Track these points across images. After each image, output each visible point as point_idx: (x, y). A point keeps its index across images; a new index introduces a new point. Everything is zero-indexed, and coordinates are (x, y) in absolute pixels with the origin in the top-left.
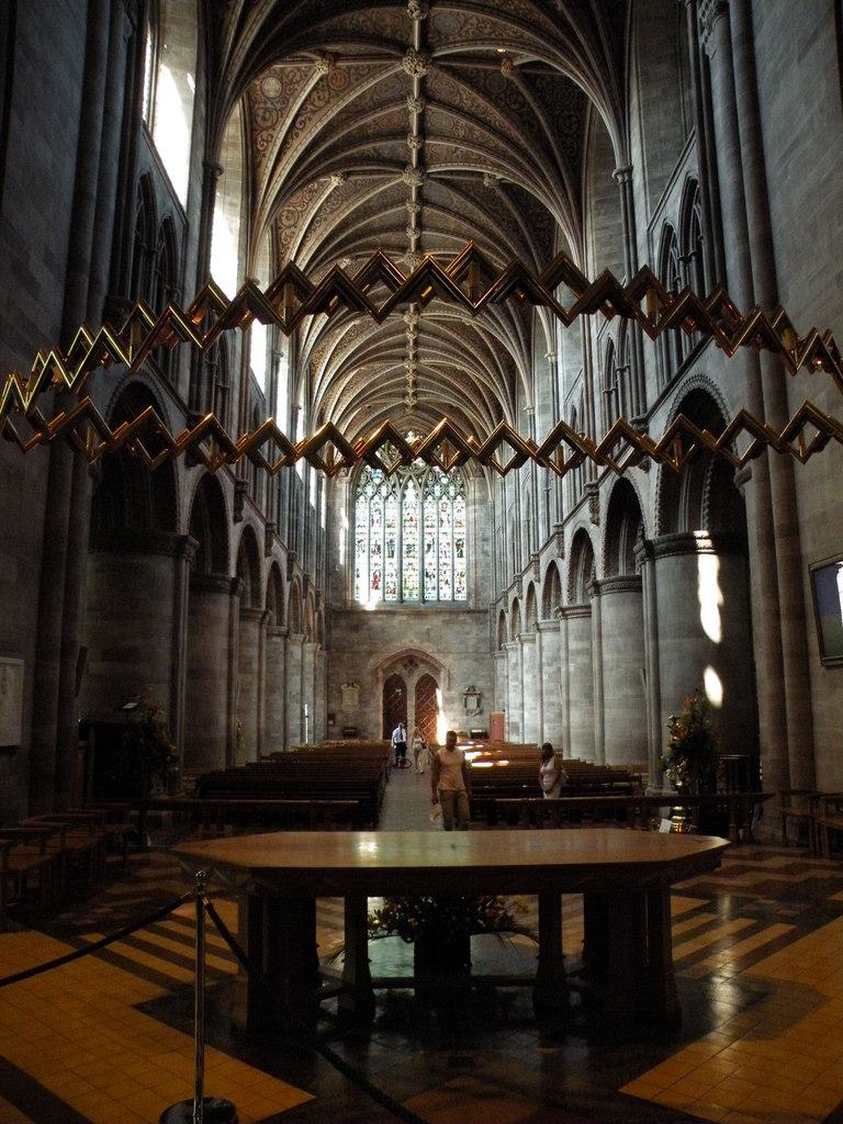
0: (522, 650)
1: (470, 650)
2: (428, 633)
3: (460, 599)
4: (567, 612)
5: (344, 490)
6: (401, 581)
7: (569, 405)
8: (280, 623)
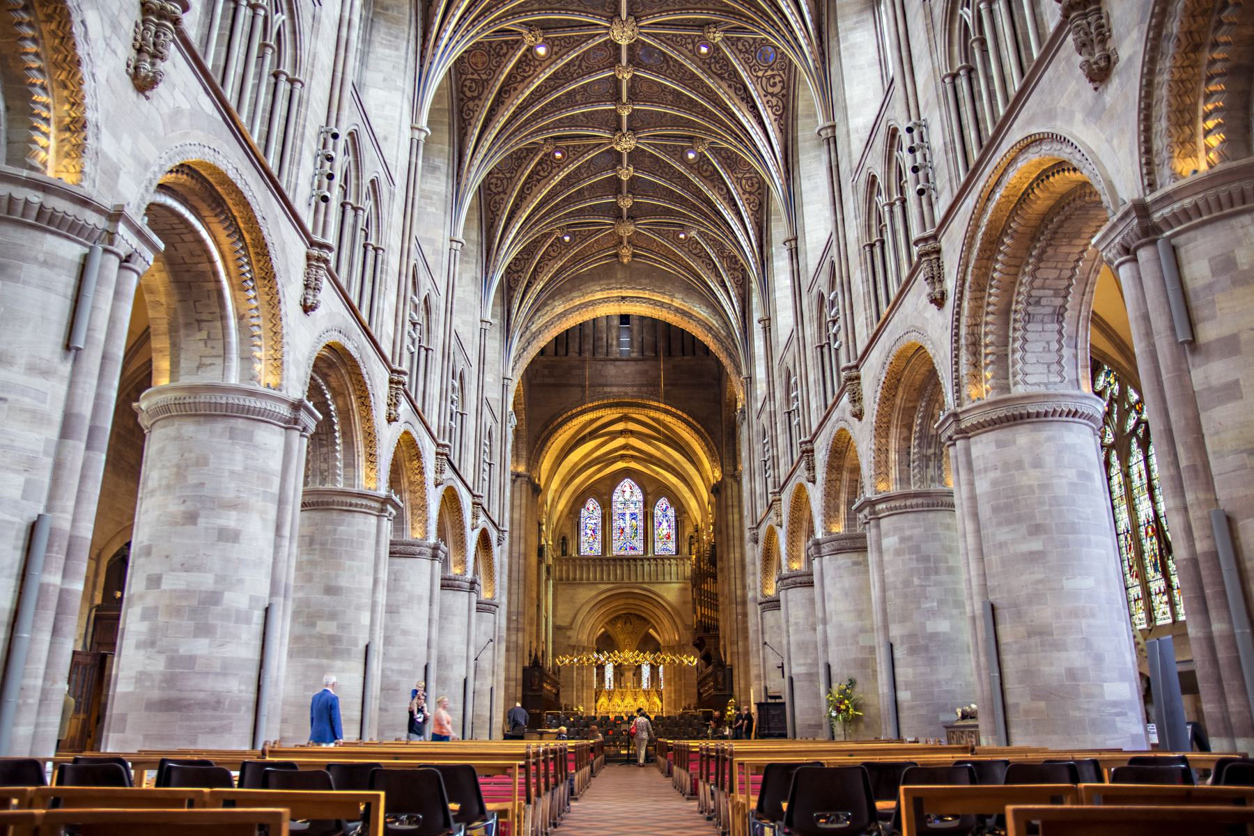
7: (815, 291)
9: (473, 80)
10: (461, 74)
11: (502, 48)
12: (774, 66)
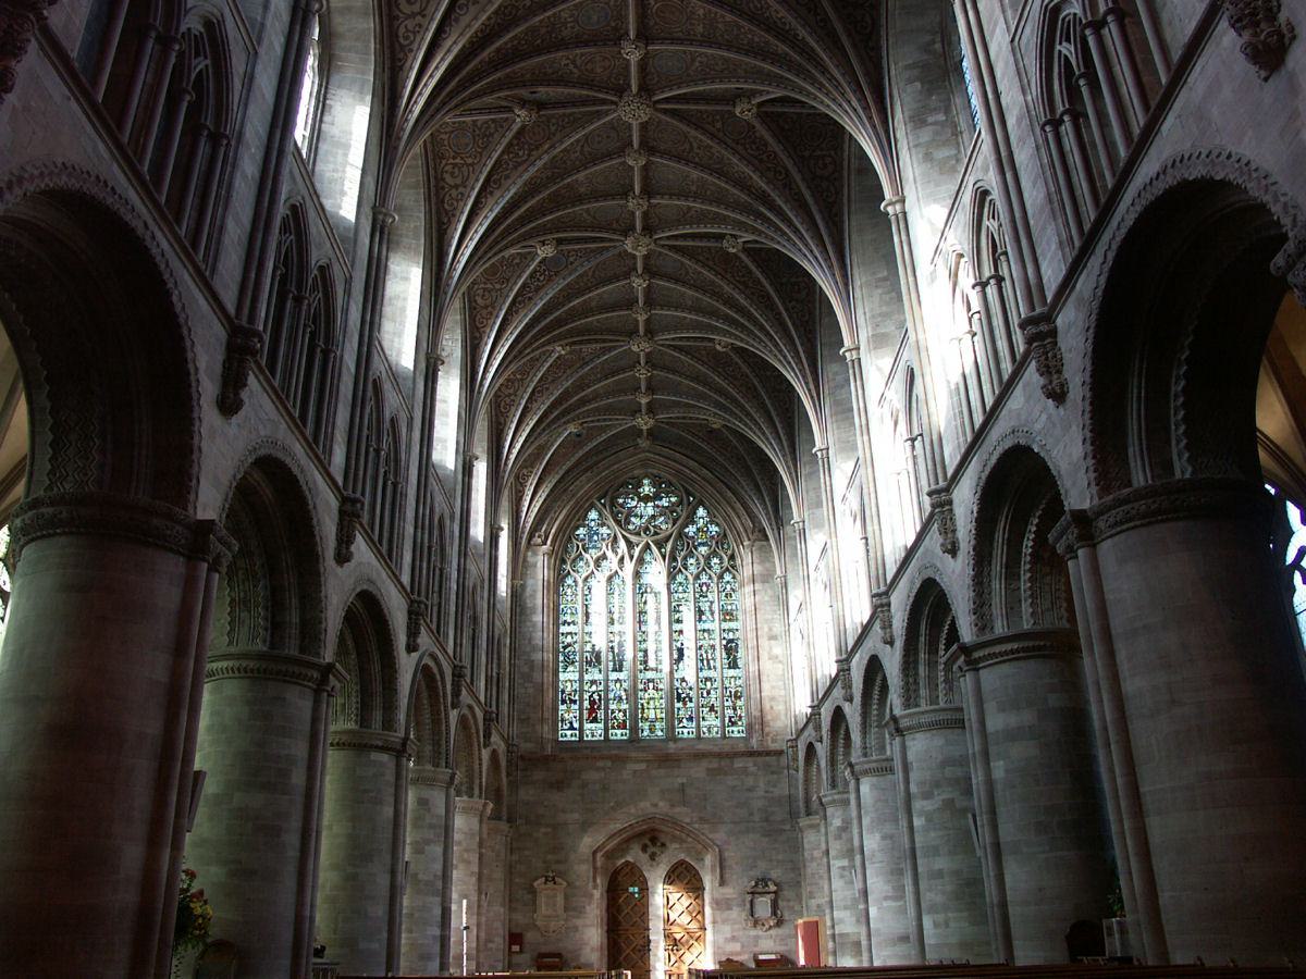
0: (858, 790)
1: (757, 818)
2: (682, 789)
3: (736, 735)
4: (976, 655)
5: (540, 564)
6: (637, 709)
8: (389, 724)
9: (455, 165)
10: (442, 157)
11: (488, 127)
12: (824, 145)
